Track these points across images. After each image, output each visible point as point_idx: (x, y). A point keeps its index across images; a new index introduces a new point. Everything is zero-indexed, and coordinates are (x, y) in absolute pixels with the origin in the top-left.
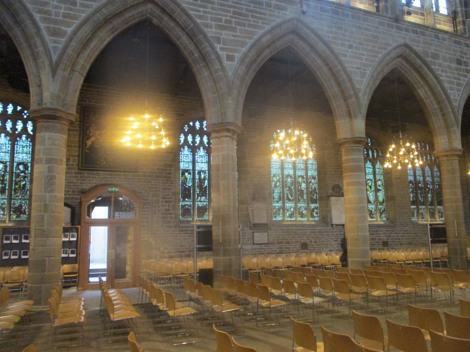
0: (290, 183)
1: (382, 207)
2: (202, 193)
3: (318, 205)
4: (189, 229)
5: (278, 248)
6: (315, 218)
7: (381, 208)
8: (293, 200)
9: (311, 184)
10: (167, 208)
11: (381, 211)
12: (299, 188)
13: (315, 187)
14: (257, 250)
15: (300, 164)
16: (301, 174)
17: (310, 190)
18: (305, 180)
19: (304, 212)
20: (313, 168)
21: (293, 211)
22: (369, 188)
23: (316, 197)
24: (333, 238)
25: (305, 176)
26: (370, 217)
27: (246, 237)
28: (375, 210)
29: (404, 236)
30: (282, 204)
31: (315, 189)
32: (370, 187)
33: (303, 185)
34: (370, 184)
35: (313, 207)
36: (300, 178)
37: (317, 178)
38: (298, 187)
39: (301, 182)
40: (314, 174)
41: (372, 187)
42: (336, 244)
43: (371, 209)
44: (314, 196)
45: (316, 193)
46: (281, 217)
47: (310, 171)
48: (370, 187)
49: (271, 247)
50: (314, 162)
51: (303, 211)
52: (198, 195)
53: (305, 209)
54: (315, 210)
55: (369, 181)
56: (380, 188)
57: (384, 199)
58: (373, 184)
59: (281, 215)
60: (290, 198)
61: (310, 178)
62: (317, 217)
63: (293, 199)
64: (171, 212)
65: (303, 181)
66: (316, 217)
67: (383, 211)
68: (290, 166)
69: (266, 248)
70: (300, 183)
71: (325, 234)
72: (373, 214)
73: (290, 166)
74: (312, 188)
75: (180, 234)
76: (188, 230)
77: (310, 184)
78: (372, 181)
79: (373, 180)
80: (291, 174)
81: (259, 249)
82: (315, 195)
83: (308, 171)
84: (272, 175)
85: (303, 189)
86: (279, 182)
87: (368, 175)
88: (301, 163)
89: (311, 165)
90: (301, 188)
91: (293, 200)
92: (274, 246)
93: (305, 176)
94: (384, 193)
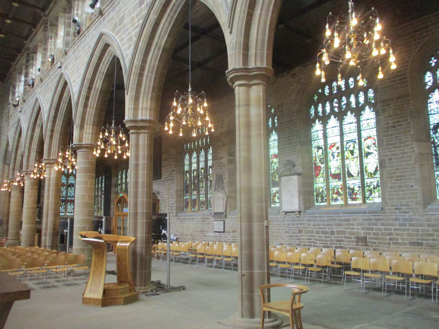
1: (372, 180)
2: (195, 188)
4: (181, 218)
5: (232, 237)
6: (277, 204)
7: (371, 182)
9: (273, 164)
10: (172, 202)
11: (372, 186)
14: (217, 238)
17: (272, 171)
22: (350, 154)
24: (285, 228)
26: (351, 198)
27: (211, 225)
28: (359, 187)
29: (404, 230)
32: (352, 152)
34: (351, 148)
35: (274, 192)
41: (355, 151)
42: (287, 237)
43: (352, 187)
44: (276, 178)
48: (352, 152)
49: (227, 236)
52: (193, 190)
54: (277, 195)
56: (369, 151)
57: (377, 168)
58: (357, 146)
61: (272, 157)
64: (174, 205)
66: (277, 203)
67: (374, 188)
69: (223, 236)
71: (275, 223)
72: (356, 194)
74: (274, 169)
75: (177, 221)
76: (180, 219)
78: (355, 142)
79: (357, 141)
81: (219, 237)
87: (348, 135)
92: (229, 235)
94: (377, 157)
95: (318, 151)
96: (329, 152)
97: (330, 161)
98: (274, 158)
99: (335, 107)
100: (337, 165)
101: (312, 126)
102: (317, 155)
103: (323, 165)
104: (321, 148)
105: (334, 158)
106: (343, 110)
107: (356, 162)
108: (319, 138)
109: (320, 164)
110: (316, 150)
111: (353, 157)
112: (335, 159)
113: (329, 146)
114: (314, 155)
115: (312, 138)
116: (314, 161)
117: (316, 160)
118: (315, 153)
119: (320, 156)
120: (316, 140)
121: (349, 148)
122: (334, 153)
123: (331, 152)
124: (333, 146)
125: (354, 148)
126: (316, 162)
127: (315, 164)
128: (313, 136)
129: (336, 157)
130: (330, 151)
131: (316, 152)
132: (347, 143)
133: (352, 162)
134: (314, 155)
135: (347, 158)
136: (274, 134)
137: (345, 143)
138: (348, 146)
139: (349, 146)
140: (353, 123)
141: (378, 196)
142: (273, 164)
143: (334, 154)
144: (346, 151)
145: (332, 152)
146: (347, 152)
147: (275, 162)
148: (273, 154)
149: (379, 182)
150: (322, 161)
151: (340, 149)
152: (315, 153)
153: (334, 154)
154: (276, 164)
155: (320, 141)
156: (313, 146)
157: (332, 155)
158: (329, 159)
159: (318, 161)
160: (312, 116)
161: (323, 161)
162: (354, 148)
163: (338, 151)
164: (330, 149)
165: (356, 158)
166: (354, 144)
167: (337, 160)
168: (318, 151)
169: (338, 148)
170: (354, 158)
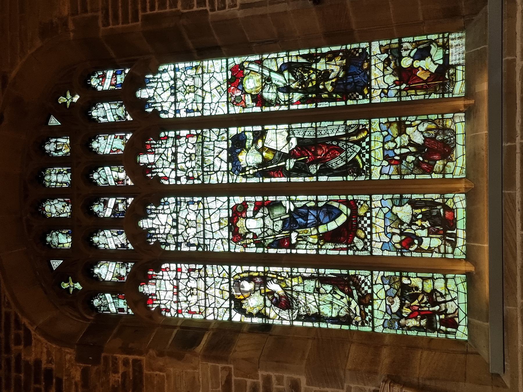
0: (268, 222)
3: (375, 47)
6: (453, 60)
8: (352, 205)
9: (269, 94)
12: (290, 164)
13: (280, 72)
15: (180, 158)
16: (224, 155)
17: (297, 96)
18: (249, 130)
19: (419, 139)
20: (190, 82)
21: (414, 204)
23: (331, 57)
25: (233, 131)
30: (378, 275)
31: (290, 67)
33: (272, 145)
35: (391, 79)
36: (242, 157)
37: (238, 60)
38: (281, 171)
39: (261, 151)
40: (221, 77)
44: (325, 75)
45: (313, 58)
46: (451, 285)
47: (208, 99)
50: (166, 77)
51: (411, 143)
53: (402, 129)
54: (406, 63)
59: (440, 285)
60: (342, 220)
61: (238, 102)
62: (445, 47)
63: (346, 203)
65: (255, 142)
66: (446, 57)
68: (192, 216)
70: (265, 162)
73: (192, 216)
74: (287, 89)
77: (269, 103)
80: (224, 213)
82: (321, 66)
83: (207, 113)
84: (237, 317)
85: (294, 142)
86: (265, 279)
88: (175, 154)
89: (180, 96)
90: (291, 155)
91: (352, 205)
93: (233, 131)
98: (243, 90)
136: (151, 92)
142: (265, 95)
147: (259, 84)
148: (224, 98)
154: (269, 79)
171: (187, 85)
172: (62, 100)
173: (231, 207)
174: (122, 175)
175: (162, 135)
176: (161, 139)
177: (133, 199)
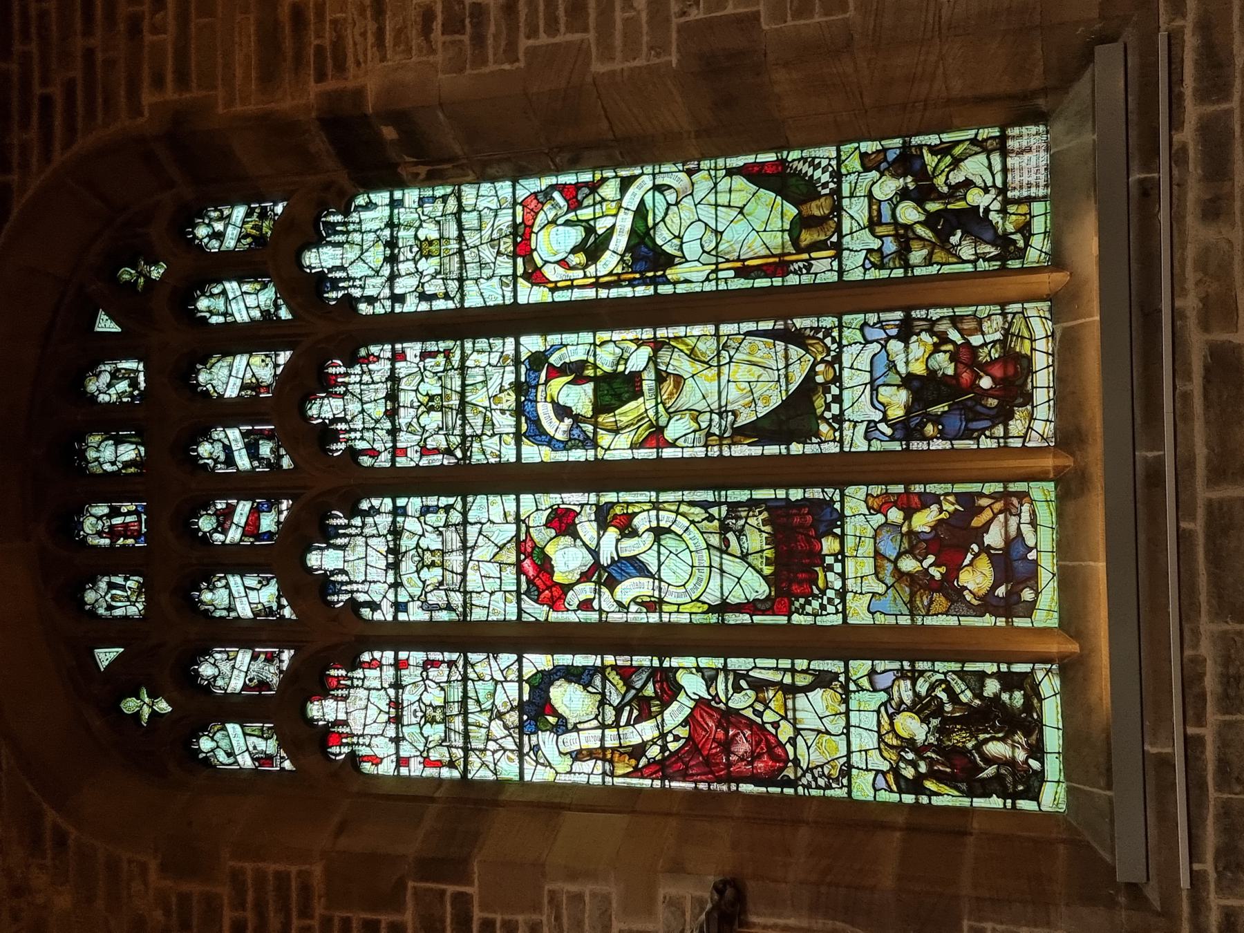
1: (857, 210)
7: (873, 224)
11: (909, 213)
22: (630, 411)
26: (1005, 416)
28: (906, 332)
34: (580, 398)
41: (606, 359)
43: (897, 400)
55: (545, 411)
56: (619, 242)
57: (755, 175)
67: (922, 194)
72: (966, 356)
78: (538, 360)
79: (532, 343)
94: (673, 176)
95: (562, 726)
96: (586, 605)
97: (654, 605)
99: (251, 527)
100: (695, 538)
101: (354, 760)
102: (589, 739)
103: (683, 678)
104: (543, 682)
105: (636, 566)
106: (286, 463)
107: (692, 355)
108: (456, 694)
109: (675, 714)
110: (546, 740)
111: (648, 384)
112: (650, 560)
113: (536, 611)
114: (590, 773)
115: (446, 773)
116: (637, 772)
117: (638, 751)
118: (578, 756)
119: (603, 702)
120: (466, 736)
121: (577, 419)
122: (597, 565)
123: (585, 591)
124: (545, 566)
125: (577, 372)
126: (654, 752)
127: (661, 768)
128: (427, 762)
129: (630, 547)
130: (573, 598)
131: (572, 741)
132: (538, 434)
133: (690, 397)
134: (587, 766)
135: (656, 436)
137: (533, 453)
138: (557, 428)
139: (562, 411)
140: (393, 378)
141: (996, 159)
143: (605, 560)
144: (596, 445)
145: (585, 577)
146: (605, 439)
149: (868, 147)
150: (649, 691)
151: (573, 499)
152: (578, 756)
153: (605, 560)
155: (483, 689)
156: (509, 770)
157: (612, 584)
158: (638, 616)
159: (647, 730)
160: (269, 759)
161: (653, 672)
162: (577, 372)
163: (588, 529)
164: (555, 594)
165: (664, 355)
166: (555, 372)
167: (659, 532)
168: (562, 726)
169: (563, 522)
170: (660, 378)
171: (428, 703)
172: (130, 705)
173: (525, 678)
174: (270, 746)
175: (366, 657)
176: (362, 665)
177: (292, 652)
